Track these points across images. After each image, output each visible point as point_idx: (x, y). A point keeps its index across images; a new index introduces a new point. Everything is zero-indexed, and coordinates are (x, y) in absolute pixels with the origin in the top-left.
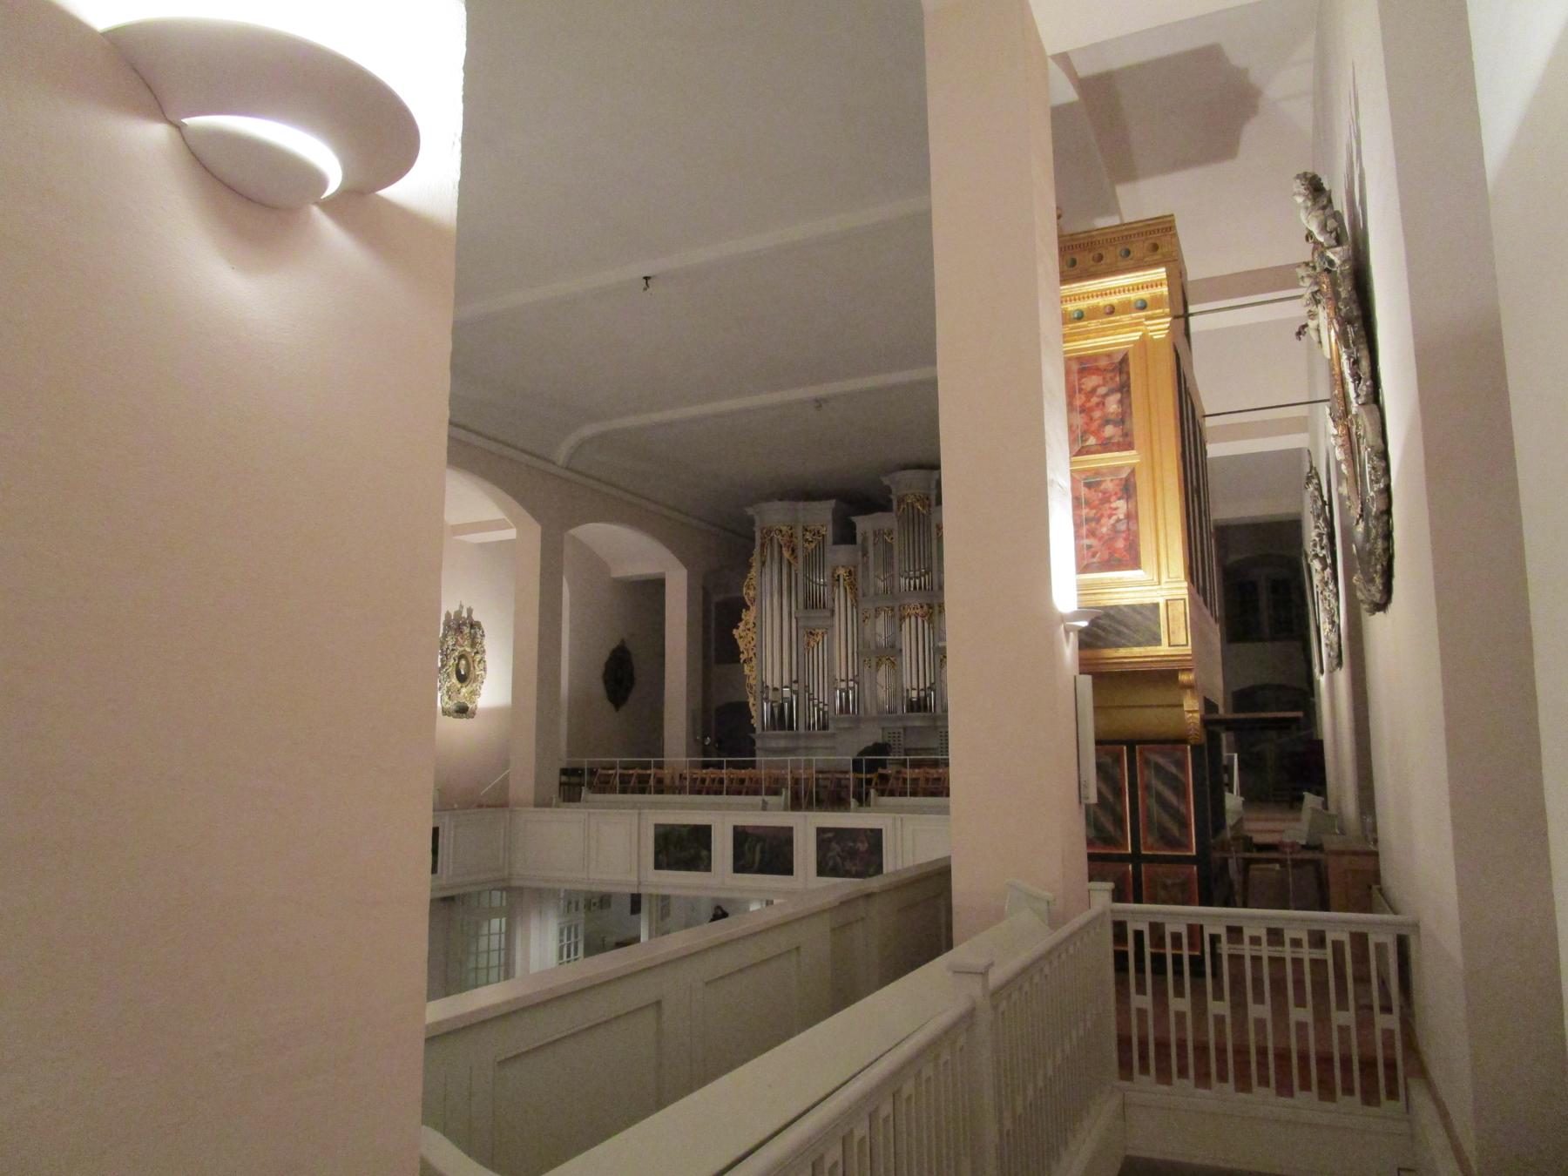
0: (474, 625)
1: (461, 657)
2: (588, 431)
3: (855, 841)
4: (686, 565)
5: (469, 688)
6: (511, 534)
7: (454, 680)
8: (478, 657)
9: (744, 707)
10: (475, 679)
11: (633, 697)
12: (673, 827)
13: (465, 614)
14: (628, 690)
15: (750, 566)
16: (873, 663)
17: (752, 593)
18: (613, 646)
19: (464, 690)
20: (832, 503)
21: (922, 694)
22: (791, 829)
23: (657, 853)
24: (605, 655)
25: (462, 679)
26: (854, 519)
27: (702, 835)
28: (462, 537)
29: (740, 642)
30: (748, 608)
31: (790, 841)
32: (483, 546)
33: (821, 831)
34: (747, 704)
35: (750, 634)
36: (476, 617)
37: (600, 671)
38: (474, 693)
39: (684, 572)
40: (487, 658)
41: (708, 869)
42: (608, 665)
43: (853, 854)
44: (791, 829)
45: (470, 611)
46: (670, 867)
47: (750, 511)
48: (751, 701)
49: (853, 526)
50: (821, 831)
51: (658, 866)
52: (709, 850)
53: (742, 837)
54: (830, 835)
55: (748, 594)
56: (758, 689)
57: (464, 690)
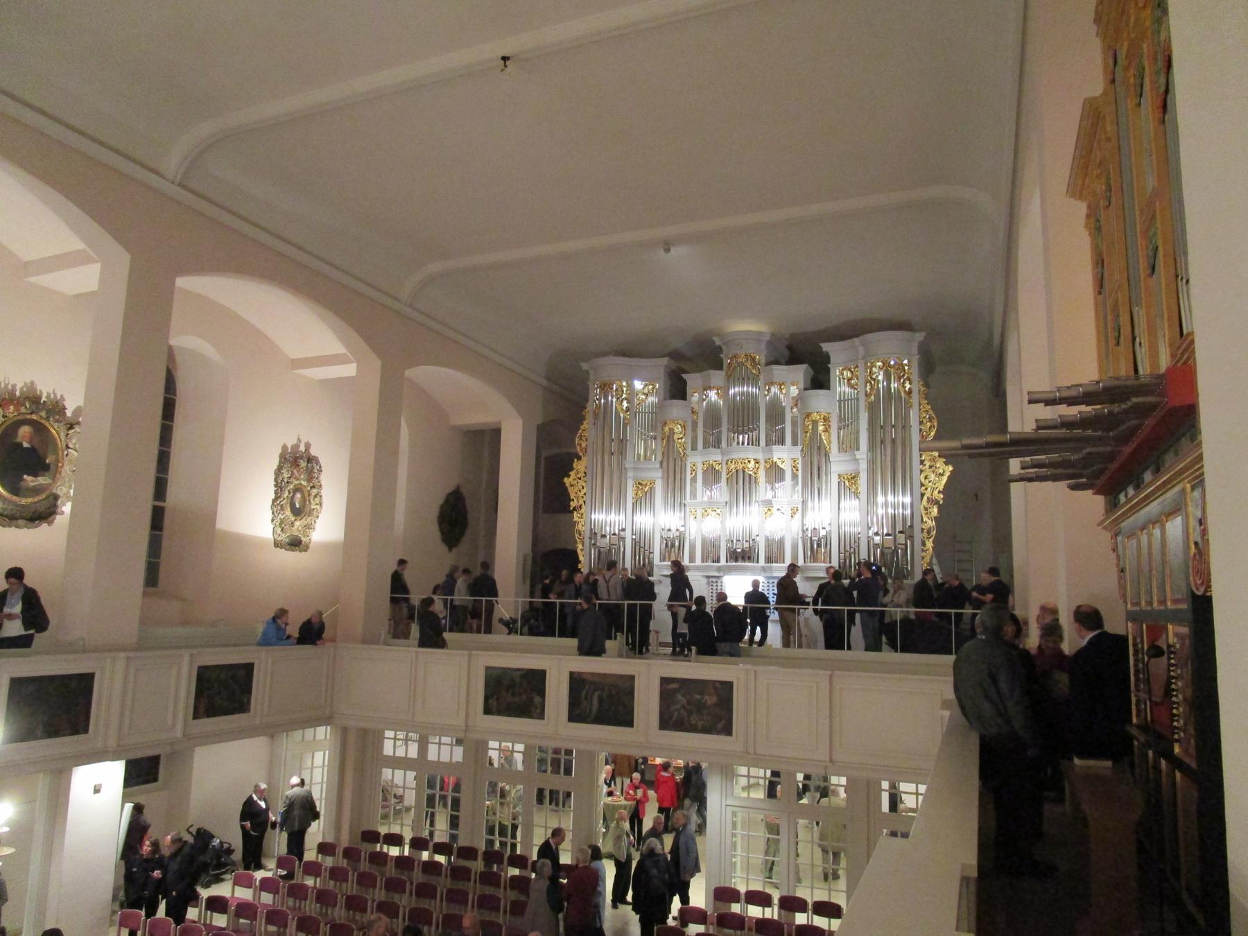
0: (311, 460)
1: (296, 490)
2: (434, 267)
3: (702, 693)
4: (522, 417)
5: (304, 522)
6: (349, 370)
7: (288, 512)
8: (314, 491)
9: (574, 554)
10: (310, 513)
12: (505, 670)
13: (302, 448)
14: (462, 534)
15: (581, 419)
17: (584, 445)
18: (449, 490)
19: (297, 523)
20: (665, 361)
21: (746, 545)
22: (632, 678)
24: (440, 500)
25: (297, 512)
27: (535, 680)
28: (301, 372)
29: (570, 490)
30: (579, 458)
31: (631, 692)
32: (325, 383)
33: (665, 681)
34: (576, 552)
35: (581, 483)
36: (313, 452)
37: (434, 512)
38: (309, 527)
39: (520, 422)
40: (323, 492)
41: (541, 716)
42: (442, 507)
43: (700, 707)
44: (632, 678)
45: (308, 446)
47: (585, 366)
48: (580, 546)
49: (685, 382)
50: (665, 681)
51: (487, 711)
54: (674, 686)
55: (580, 444)
56: (587, 534)
57: (297, 523)
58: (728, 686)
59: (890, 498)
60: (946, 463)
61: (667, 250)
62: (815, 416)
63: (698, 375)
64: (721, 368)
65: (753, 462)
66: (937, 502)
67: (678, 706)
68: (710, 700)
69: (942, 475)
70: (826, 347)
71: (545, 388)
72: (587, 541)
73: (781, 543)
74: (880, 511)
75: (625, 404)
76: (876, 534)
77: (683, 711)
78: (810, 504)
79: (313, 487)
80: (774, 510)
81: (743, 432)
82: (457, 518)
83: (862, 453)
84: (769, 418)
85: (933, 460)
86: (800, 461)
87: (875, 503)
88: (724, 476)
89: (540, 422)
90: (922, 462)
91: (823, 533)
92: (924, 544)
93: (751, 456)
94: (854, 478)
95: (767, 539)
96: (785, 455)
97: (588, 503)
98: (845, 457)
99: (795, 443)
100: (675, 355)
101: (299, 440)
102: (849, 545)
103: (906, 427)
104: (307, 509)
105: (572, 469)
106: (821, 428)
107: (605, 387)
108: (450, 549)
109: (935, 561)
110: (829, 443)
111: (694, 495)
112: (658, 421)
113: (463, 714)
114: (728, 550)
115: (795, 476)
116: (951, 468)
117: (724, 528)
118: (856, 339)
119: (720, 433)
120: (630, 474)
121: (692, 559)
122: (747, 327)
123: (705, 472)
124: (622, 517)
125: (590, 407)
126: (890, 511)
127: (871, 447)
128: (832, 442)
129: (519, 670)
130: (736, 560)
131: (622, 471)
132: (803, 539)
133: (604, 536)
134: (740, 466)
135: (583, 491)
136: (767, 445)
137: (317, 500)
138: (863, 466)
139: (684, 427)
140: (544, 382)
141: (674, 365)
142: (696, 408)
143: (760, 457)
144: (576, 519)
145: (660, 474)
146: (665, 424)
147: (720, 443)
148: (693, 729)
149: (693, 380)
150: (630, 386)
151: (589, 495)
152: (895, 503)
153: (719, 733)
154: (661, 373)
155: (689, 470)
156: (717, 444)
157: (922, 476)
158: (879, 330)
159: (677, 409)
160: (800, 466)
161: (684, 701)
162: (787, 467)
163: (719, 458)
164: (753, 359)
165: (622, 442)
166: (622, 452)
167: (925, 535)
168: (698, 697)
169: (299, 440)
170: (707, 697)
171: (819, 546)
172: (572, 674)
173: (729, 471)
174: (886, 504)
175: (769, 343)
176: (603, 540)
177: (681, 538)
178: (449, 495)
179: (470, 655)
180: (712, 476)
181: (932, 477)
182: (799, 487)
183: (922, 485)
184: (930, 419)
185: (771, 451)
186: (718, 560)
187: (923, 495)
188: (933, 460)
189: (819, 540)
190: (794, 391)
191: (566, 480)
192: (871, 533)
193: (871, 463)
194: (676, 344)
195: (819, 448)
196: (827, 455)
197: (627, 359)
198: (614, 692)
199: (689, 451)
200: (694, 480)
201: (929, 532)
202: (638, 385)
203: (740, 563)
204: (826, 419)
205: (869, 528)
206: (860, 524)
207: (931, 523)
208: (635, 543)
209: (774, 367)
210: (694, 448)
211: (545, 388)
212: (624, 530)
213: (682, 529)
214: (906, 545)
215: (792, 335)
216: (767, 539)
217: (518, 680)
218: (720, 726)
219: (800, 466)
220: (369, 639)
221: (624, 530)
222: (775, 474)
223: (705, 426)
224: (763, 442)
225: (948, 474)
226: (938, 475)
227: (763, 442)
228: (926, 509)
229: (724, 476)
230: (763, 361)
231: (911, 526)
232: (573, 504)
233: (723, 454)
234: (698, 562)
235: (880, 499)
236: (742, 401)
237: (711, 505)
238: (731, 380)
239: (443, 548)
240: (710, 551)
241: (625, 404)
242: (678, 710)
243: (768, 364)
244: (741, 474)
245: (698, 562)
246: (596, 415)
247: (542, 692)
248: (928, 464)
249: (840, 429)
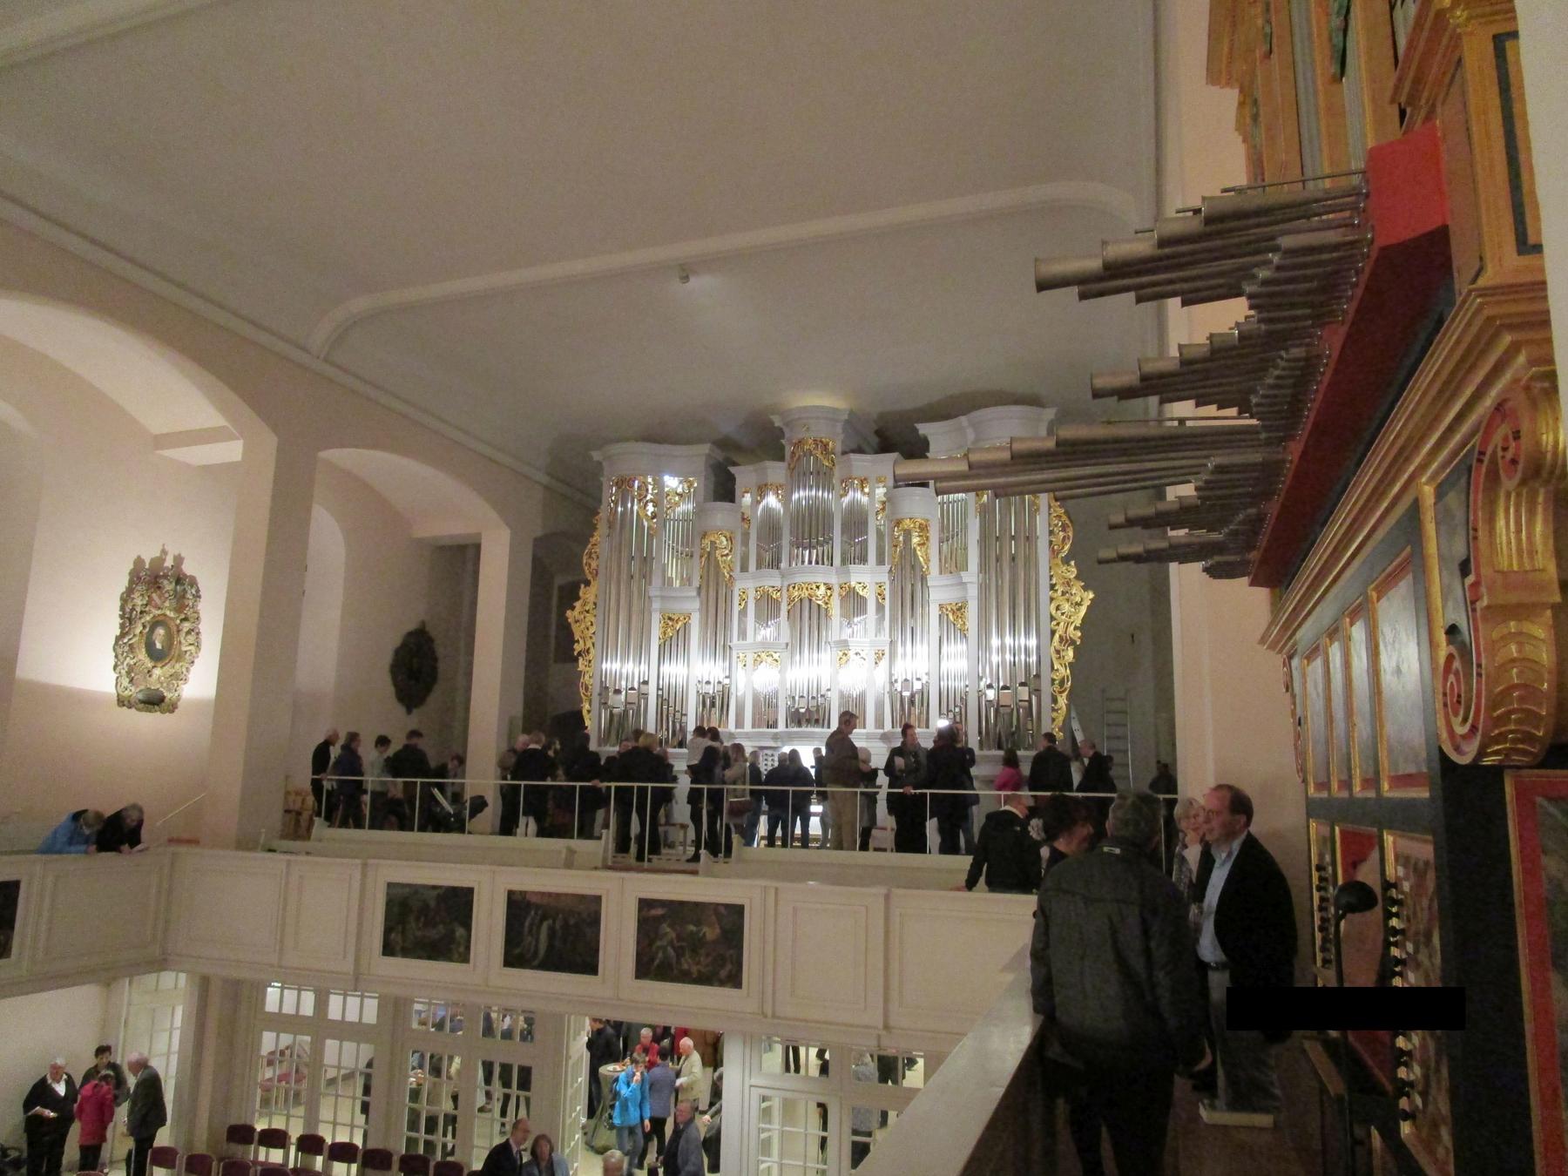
0: (180, 579)
1: (155, 624)
2: (361, 304)
3: (698, 923)
4: (511, 528)
5: (168, 669)
6: (232, 451)
7: (142, 655)
8: (186, 626)
9: (577, 718)
10: (180, 657)
11: (435, 699)
12: (415, 889)
13: (169, 563)
14: (428, 689)
15: (594, 528)
16: (750, 661)
17: (594, 565)
18: (411, 626)
19: (157, 672)
20: (705, 448)
22: (598, 899)
23: (388, 931)
24: (394, 640)
25: (157, 656)
26: (732, 469)
27: (458, 902)
28: (167, 453)
29: (575, 627)
30: (588, 583)
31: (595, 921)
32: (208, 470)
33: (645, 904)
34: (580, 712)
35: (589, 617)
36: (188, 569)
37: (387, 659)
38: (177, 677)
40: (202, 627)
41: (465, 958)
42: (397, 652)
43: (696, 945)
44: (598, 899)
45: (179, 560)
46: (407, 952)
47: (596, 456)
48: (586, 706)
49: (732, 479)
50: (645, 904)
51: (388, 950)
52: (467, 925)
53: (518, 905)
54: (659, 912)
55: (590, 564)
56: (597, 690)
57: (157, 672)
58: (735, 913)
59: (1008, 640)
60: (1085, 588)
61: (685, 279)
62: (907, 524)
63: (751, 468)
64: (782, 459)
65: (823, 588)
66: (1073, 642)
67: (664, 943)
68: (711, 932)
69: (1079, 604)
70: (924, 429)
71: (547, 488)
72: (596, 699)
73: (861, 700)
74: (995, 659)
75: (650, 508)
76: (990, 686)
77: (670, 949)
78: (900, 650)
79: (186, 619)
80: (851, 653)
81: (811, 547)
82: (420, 667)
83: (972, 575)
84: (846, 528)
86: (887, 586)
87: (988, 648)
88: (784, 608)
89: (539, 533)
90: (1052, 587)
91: (917, 686)
92: (1055, 701)
93: (820, 579)
94: (960, 609)
95: (842, 695)
96: (868, 578)
97: (599, 645)
98: (947, 580)
99: (880, 561)
100: (724, 444)
101: (164, 552)
102: (955, 704)
103: (1030, 539)
104: (175, 652)
105: (578, 598)
106: (915, 540)
107: (624, 484)
108: (409, 711)
109: (1075, 725)
110: (927, 560)
111: (743, 634)
112: (695, 535)
113: (351, 958)
114: (788, 708)
115: (880, 608)
116: (1091, 595)
117: (783, 681)
118: (963, 419)
119: (779, 548)
120: (656, 605)
121: (739, 724)
122: (817, 403)
123: (757, 601)
124: (644, 667)
125: (603, 514)
126: (1008, 657)
127: (984, 567)
128: (930, 556)
129: (434, 887)
130: (799, 724)
131: (646, 599)
132: (890, 693)
133: (618, 692)
134: (805, 594)
135: (592, 630)
136: (844, 562)
137: (191, 639)
138: (973, 592)
139: (730, 539)
140: (545, 479)
141: (719, 456)
142: (748, 513)
144: (581, 667)
145: (696, 604)
146: (704, 536)
147: (779, 561)
148: (685, 977)
149: (744, 475)
150: (659, 484)
151: (599, 634)
152: (1014, 647)
153: (722, 983)
154: (700, 464)
155: (736, 600)
156: (775, 563)
157: (1053, 606)
158: (996, 404)
159: (721, 514)
160: (887, 594)
161: (673, 935)
162: (870, 595)
163: (777, 583)
164: (825, 446)
165: (647, 561)
166: (646, 576)
167: (1057, 687)
168: (692, 928)
169: (164, 552)
170: (705, 929)
171: (912, 702)
172: (511, 893)
173: (791, 600)
174: (1002, 649)
175: (847, 422)
176: (617, 697)
177: (725, 694)
179: (365, 865)
180: (768, 607)
181: (1066, 607)
182: (887, 623)
183: (1052, 618)
185: (848, 572)
186: (775, 725)
187: (1053, 633)
189: (913, 696)
190: (880, 492)
191: (569, 613)
192: (982, 684)
193: (984, 589)
194: (728, 428)
195: (913, 567)
196: (923, 579)
197: (654, 446)
198: (572, 922)
199: (737, 573)
200: (743, 613)
201: (1062, 683)
202: (672, 482)
203: (803, 729)
204: (923, 528)
205: (980, 678)
206: (967, 676)
207: (1064, 672)
208: (662, 701)
209: (852, 456)
210: (744, 568)
211: (547, 488)
212: (646, 683)
213: (727, 681)
214: (1030, 701)
215: (882, 416)
216: (842, 695)
217: (432, 904)
218: (723, 973)
219: (887, 594)
220: (245, 843)
221: (646, 683)
222: (854, 603)
223: (759, 539)
224: (837, 560)
225: (1087, 603)
226: (1073, 606)
227: (837, 560)
228: (1058, 652)
229: (784, 608)
230: (839, 449)
231: (1038, 676)
232: (578, 647)
233: (783, 576)
234: (748, 727)
235: (995, 642)
236: (809, 507)
237: (763, 652)
238: (798, 477)
239: (400, 710)
240: (765, 710)
241: (650, 508)
242: (664, 948)
243: (844, 453)
244: (806, 604)
245: (748, 727)
246: (611, 526)
247: (466, 920)
248: (1060, 589)
249: (941, 541)
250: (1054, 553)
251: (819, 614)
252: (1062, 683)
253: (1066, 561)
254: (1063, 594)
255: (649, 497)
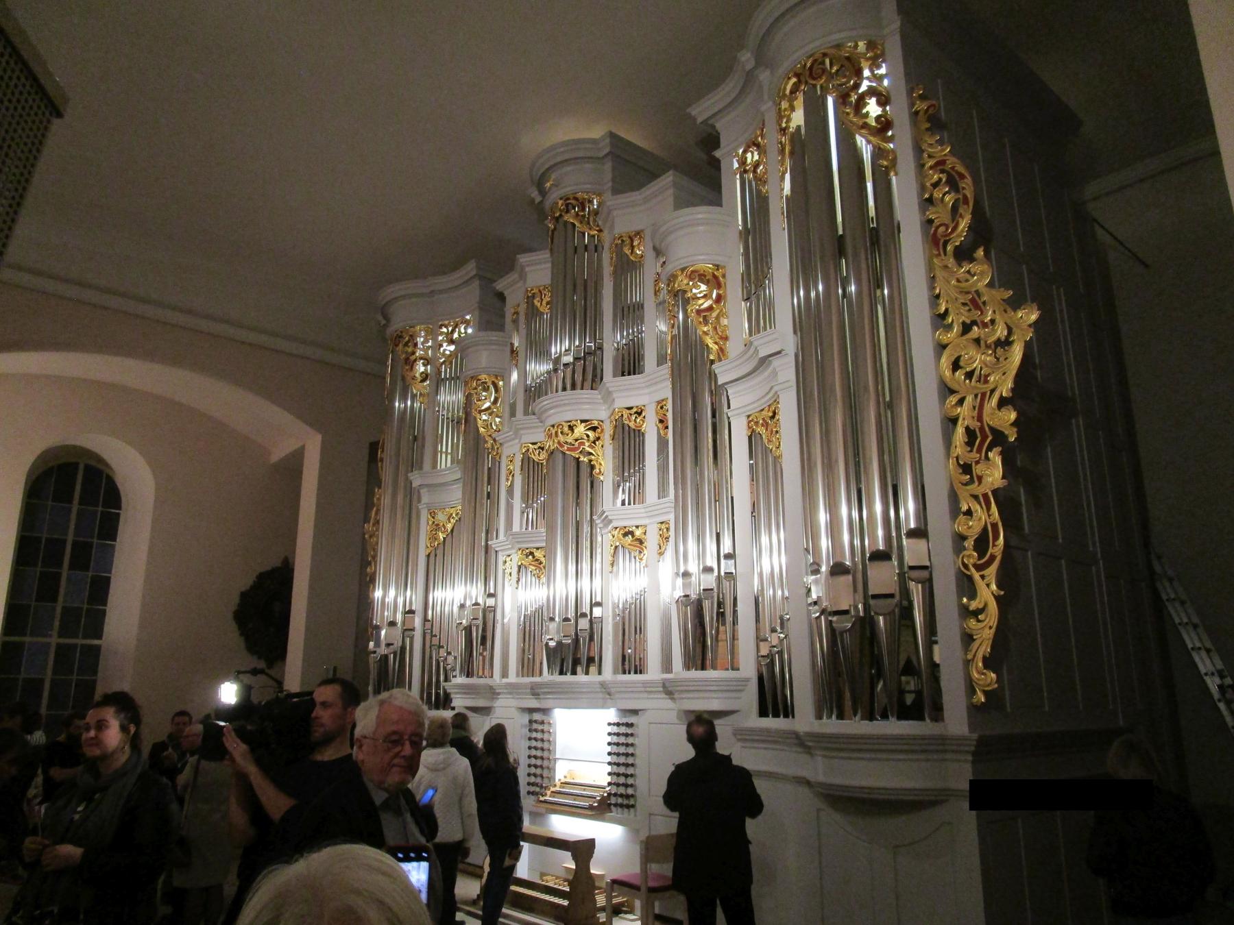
24: (245, 582)
60: (1015, 303)
66: (998, 438)
69: (1005, 343)
85: (976, 303)
86: (669, 406)
92: (966, 586)
143: (601, 413)
157: (946, 361)
167: (971, 557)
178: (262, 577)
181: (977, 359)
184: (953, 184)
188: (976, 303)
201: (982, 544)
207: (985, 516)
228: (966, 469)
250: (935, 240)
251: (582, 476)
252: (982, 544)
253: (963, 254)
254: (966, 328)
255: (419, 353)
